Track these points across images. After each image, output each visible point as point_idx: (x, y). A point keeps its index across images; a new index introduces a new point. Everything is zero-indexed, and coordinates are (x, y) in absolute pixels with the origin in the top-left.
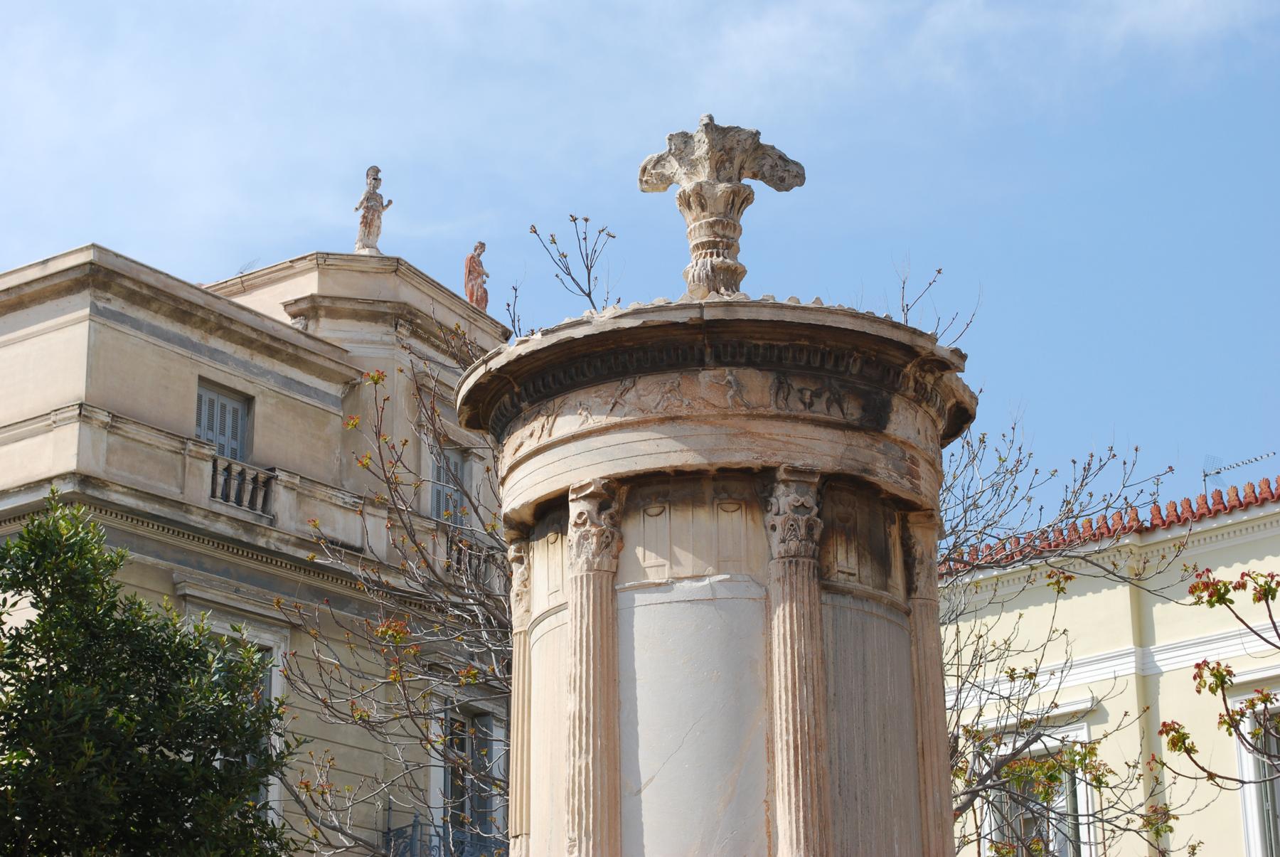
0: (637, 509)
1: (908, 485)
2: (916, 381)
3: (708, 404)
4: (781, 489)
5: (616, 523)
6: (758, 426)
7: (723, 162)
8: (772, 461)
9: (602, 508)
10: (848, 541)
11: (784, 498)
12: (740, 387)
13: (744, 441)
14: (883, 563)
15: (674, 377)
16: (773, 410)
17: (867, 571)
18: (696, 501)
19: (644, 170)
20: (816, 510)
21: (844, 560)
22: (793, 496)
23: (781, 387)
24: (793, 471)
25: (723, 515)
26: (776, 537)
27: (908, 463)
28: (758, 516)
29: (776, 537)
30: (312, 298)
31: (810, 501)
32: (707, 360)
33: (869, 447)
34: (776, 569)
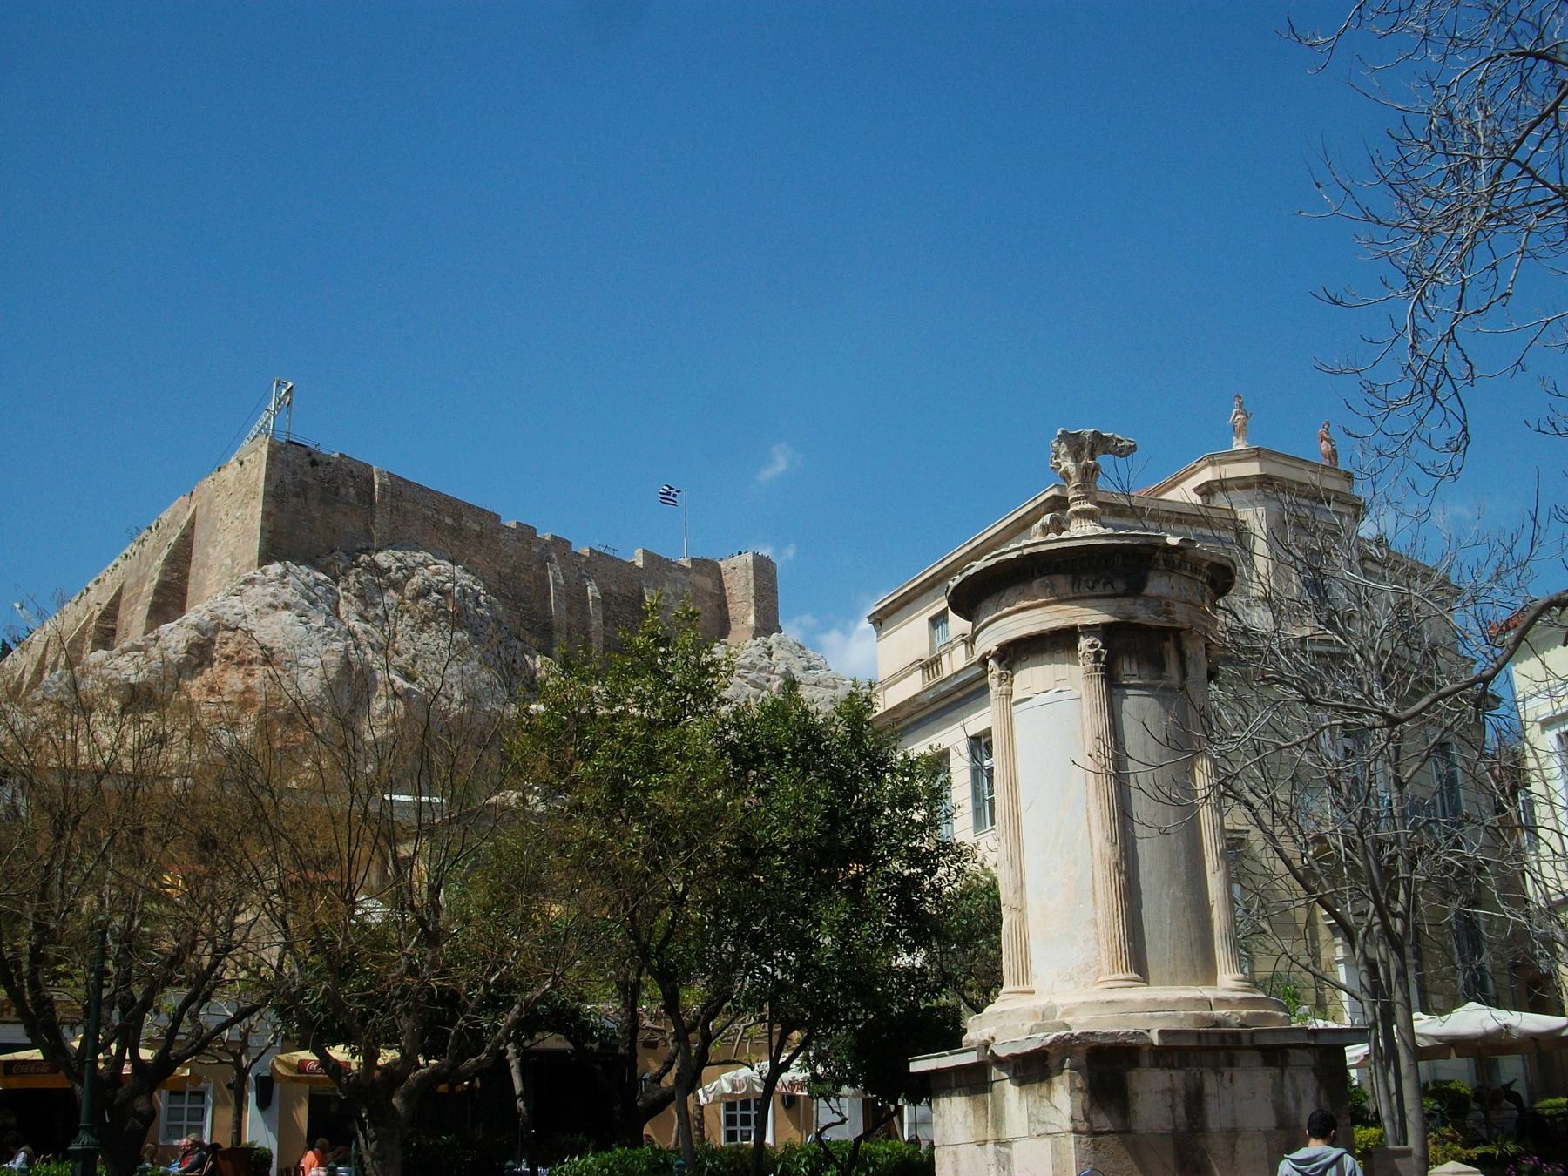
1: (1165, 619)
2: (1165, 560)
7: (1078, 452)
10: (1130, 657)
11: (1083, 643)
13: (1057, 615)
14: (1159, 664)
15: (1021, 587)
16: (1071, 595)
17: (1144, 672)
20: (1100, 644)
21: (1128, 669)
23: (1075, 583)
24: (1084, 626)
25: (1056, 655)
27: (1164, 607)
30: (1207, 483)
32: (1036, 574)
33: (1134, 604)
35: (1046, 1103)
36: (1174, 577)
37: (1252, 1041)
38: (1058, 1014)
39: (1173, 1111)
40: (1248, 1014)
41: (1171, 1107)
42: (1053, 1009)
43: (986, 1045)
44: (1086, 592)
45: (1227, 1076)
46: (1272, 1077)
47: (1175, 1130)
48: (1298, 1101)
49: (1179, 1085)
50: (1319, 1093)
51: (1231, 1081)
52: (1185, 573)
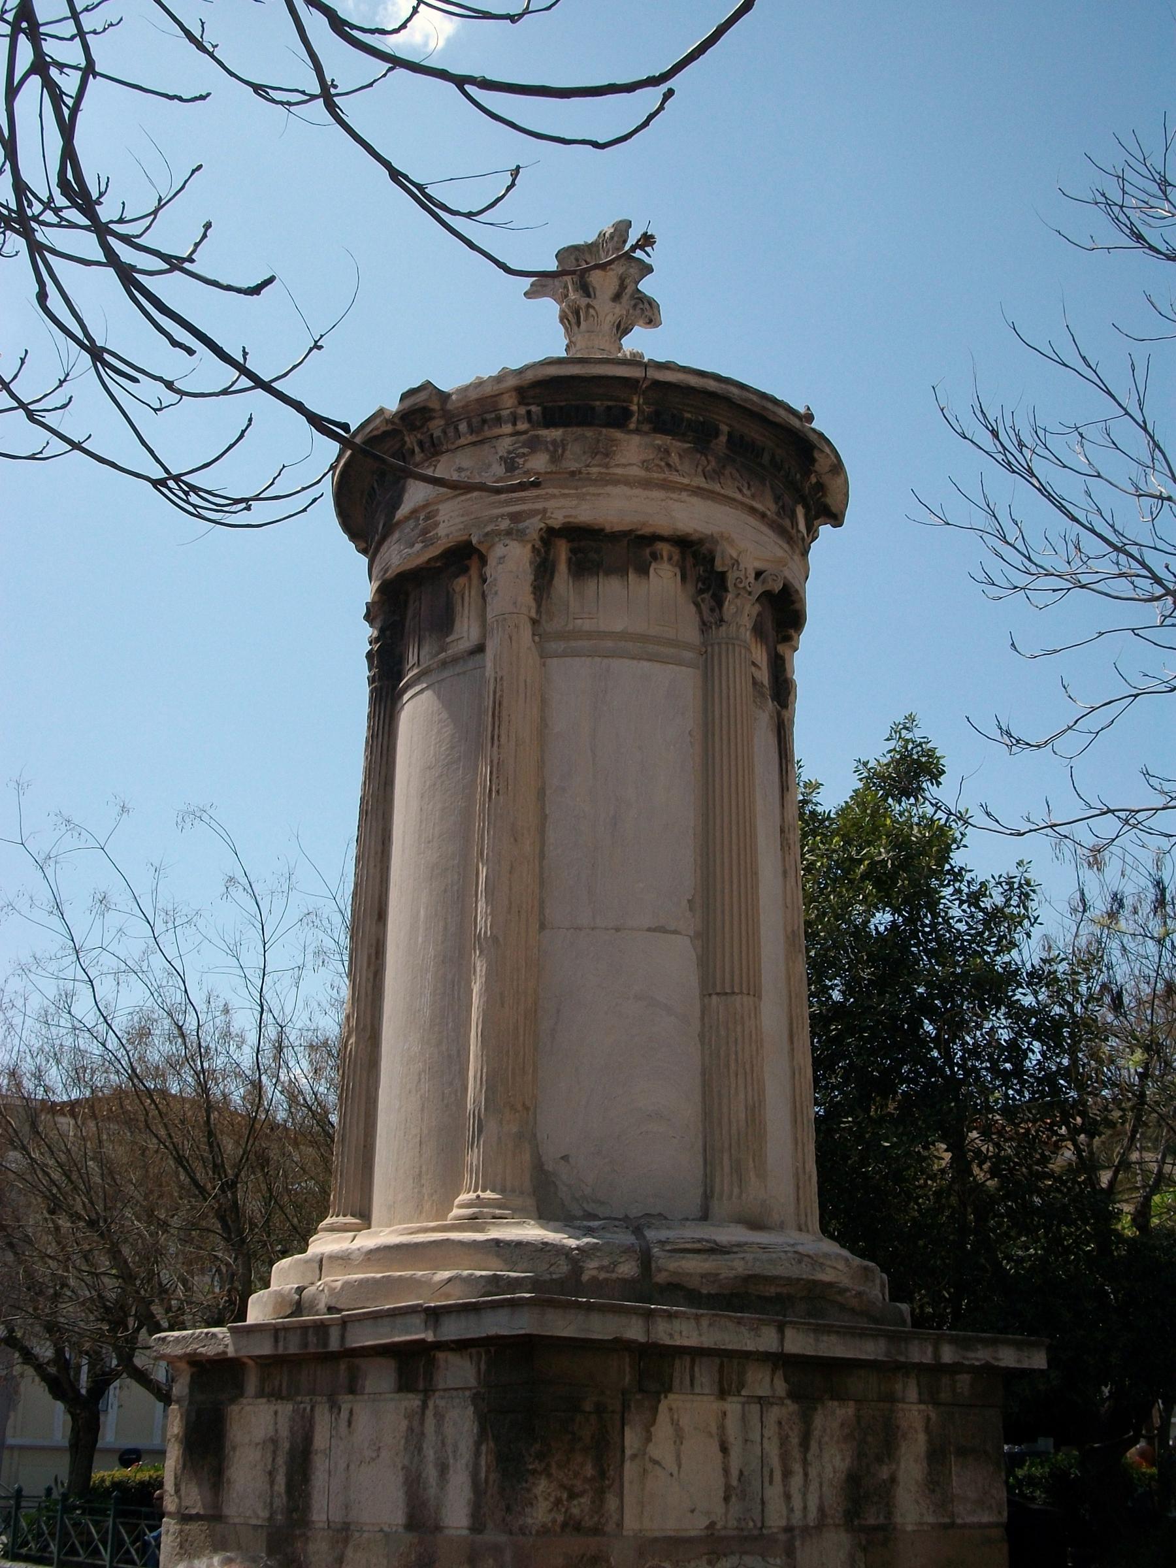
36: (444, 459)
37: (343, 1338)
39: (272, 1483)
40: (346, 1284)
41: (270, 1473)
45: (344, 1415)
46: (409, 1416)
47: (271, 1518)
48: (443, 1469)
49: (284, 1433)
50: (477, 1454)
51: (350, 1423)
52: (462, 441)
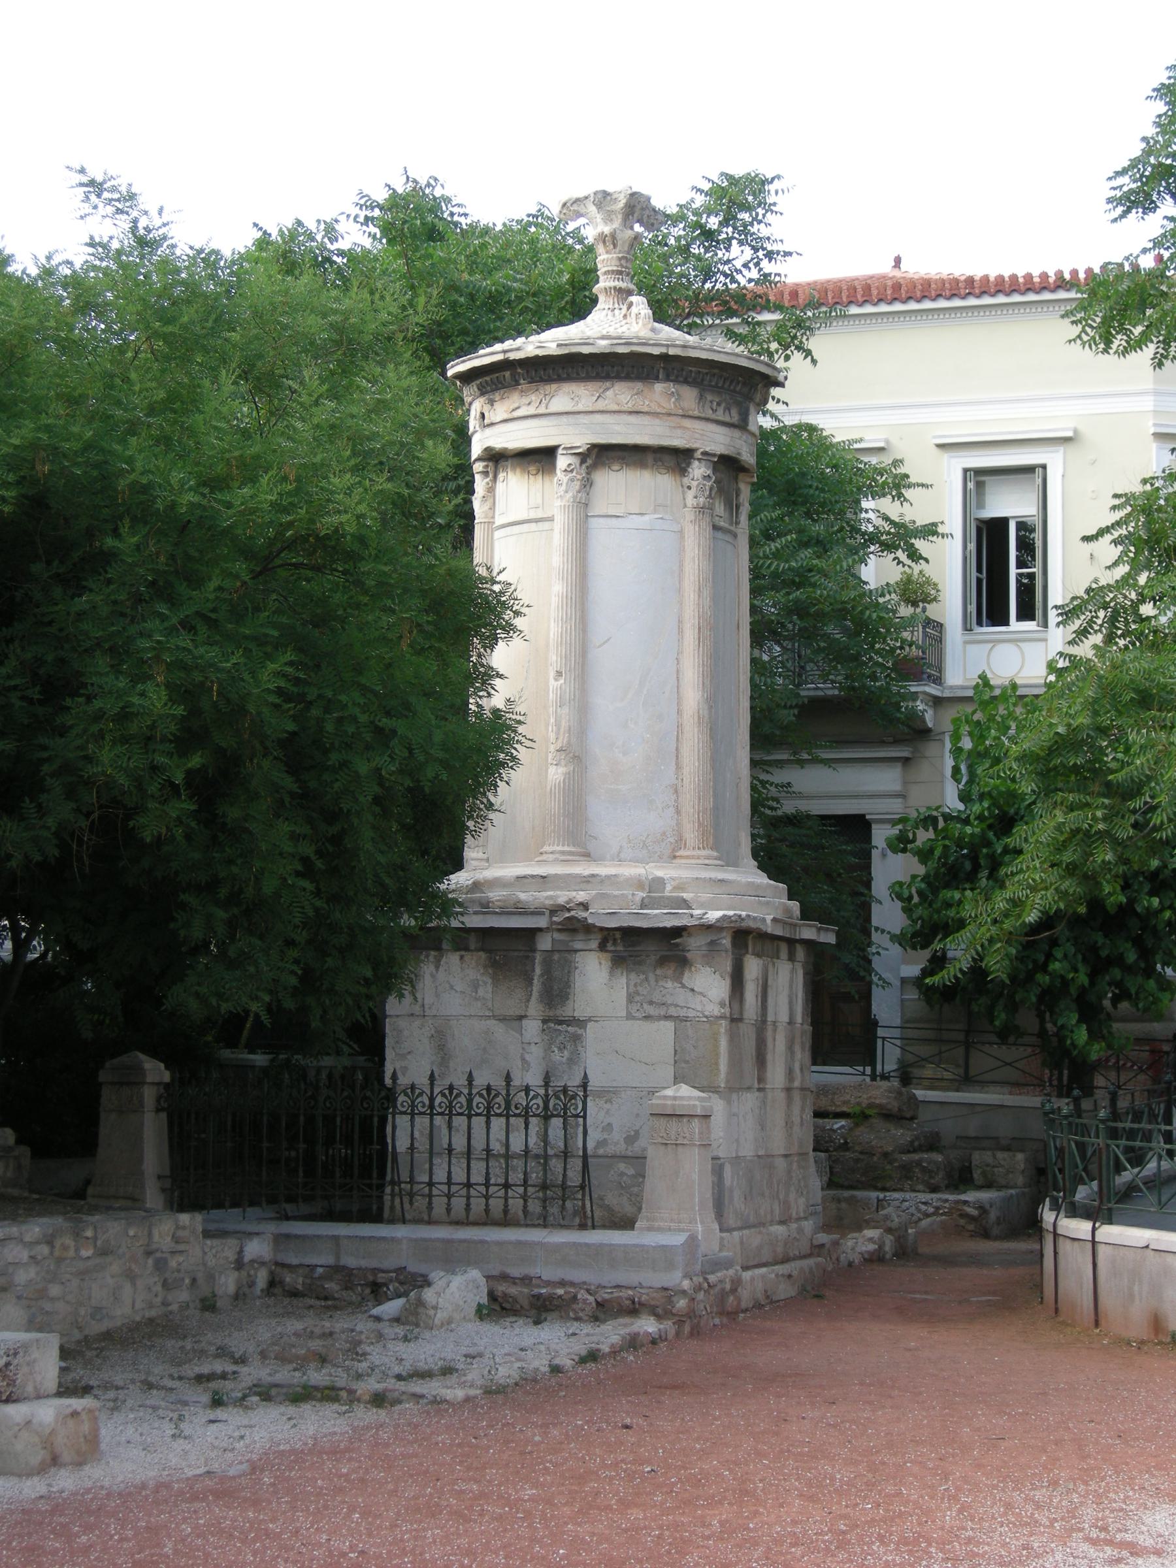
0: (603, 465)
3: (660, 405)
4: (696, 463)
5: (588, 473)
6: (687, 423)
8: (694, 446)
9: (582, 462)
12: (679, 397)
13: (679, 432)
15: (639, 385)
16: (696, 413)
18: (643, 465)
19: (564, 205)
21: (720, 509)
22: (703, 469)
23: (701, 397)
24: (705, 453)
26: (690, 495)
28: (678, 478)
29: (690, 495)
31: (709, 472)
33: (740, 438)
34: (689, 515)
35: (669, 984)
38: (668, 888)
42: (659, 883)
43: (555, 910)
44: (709, 413)
